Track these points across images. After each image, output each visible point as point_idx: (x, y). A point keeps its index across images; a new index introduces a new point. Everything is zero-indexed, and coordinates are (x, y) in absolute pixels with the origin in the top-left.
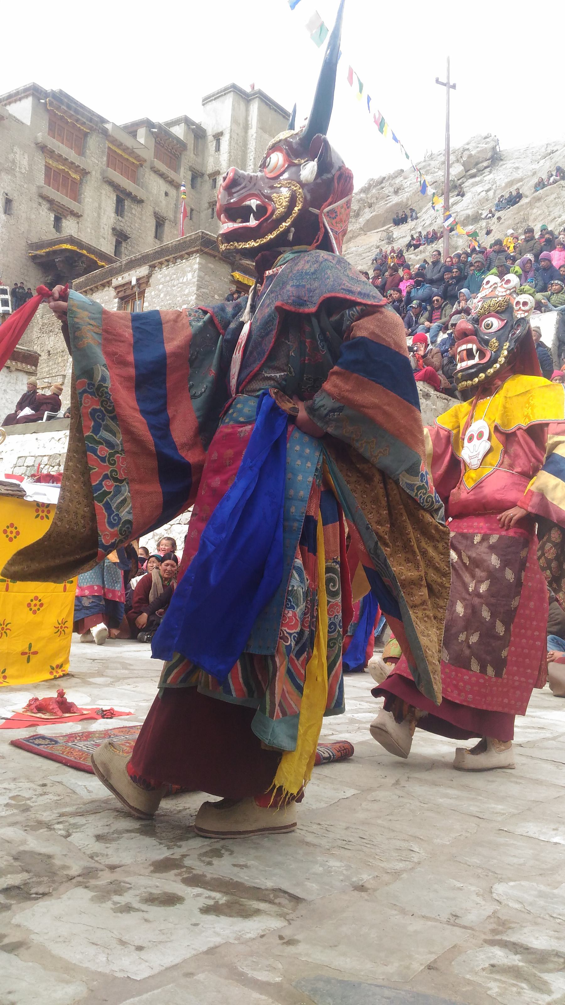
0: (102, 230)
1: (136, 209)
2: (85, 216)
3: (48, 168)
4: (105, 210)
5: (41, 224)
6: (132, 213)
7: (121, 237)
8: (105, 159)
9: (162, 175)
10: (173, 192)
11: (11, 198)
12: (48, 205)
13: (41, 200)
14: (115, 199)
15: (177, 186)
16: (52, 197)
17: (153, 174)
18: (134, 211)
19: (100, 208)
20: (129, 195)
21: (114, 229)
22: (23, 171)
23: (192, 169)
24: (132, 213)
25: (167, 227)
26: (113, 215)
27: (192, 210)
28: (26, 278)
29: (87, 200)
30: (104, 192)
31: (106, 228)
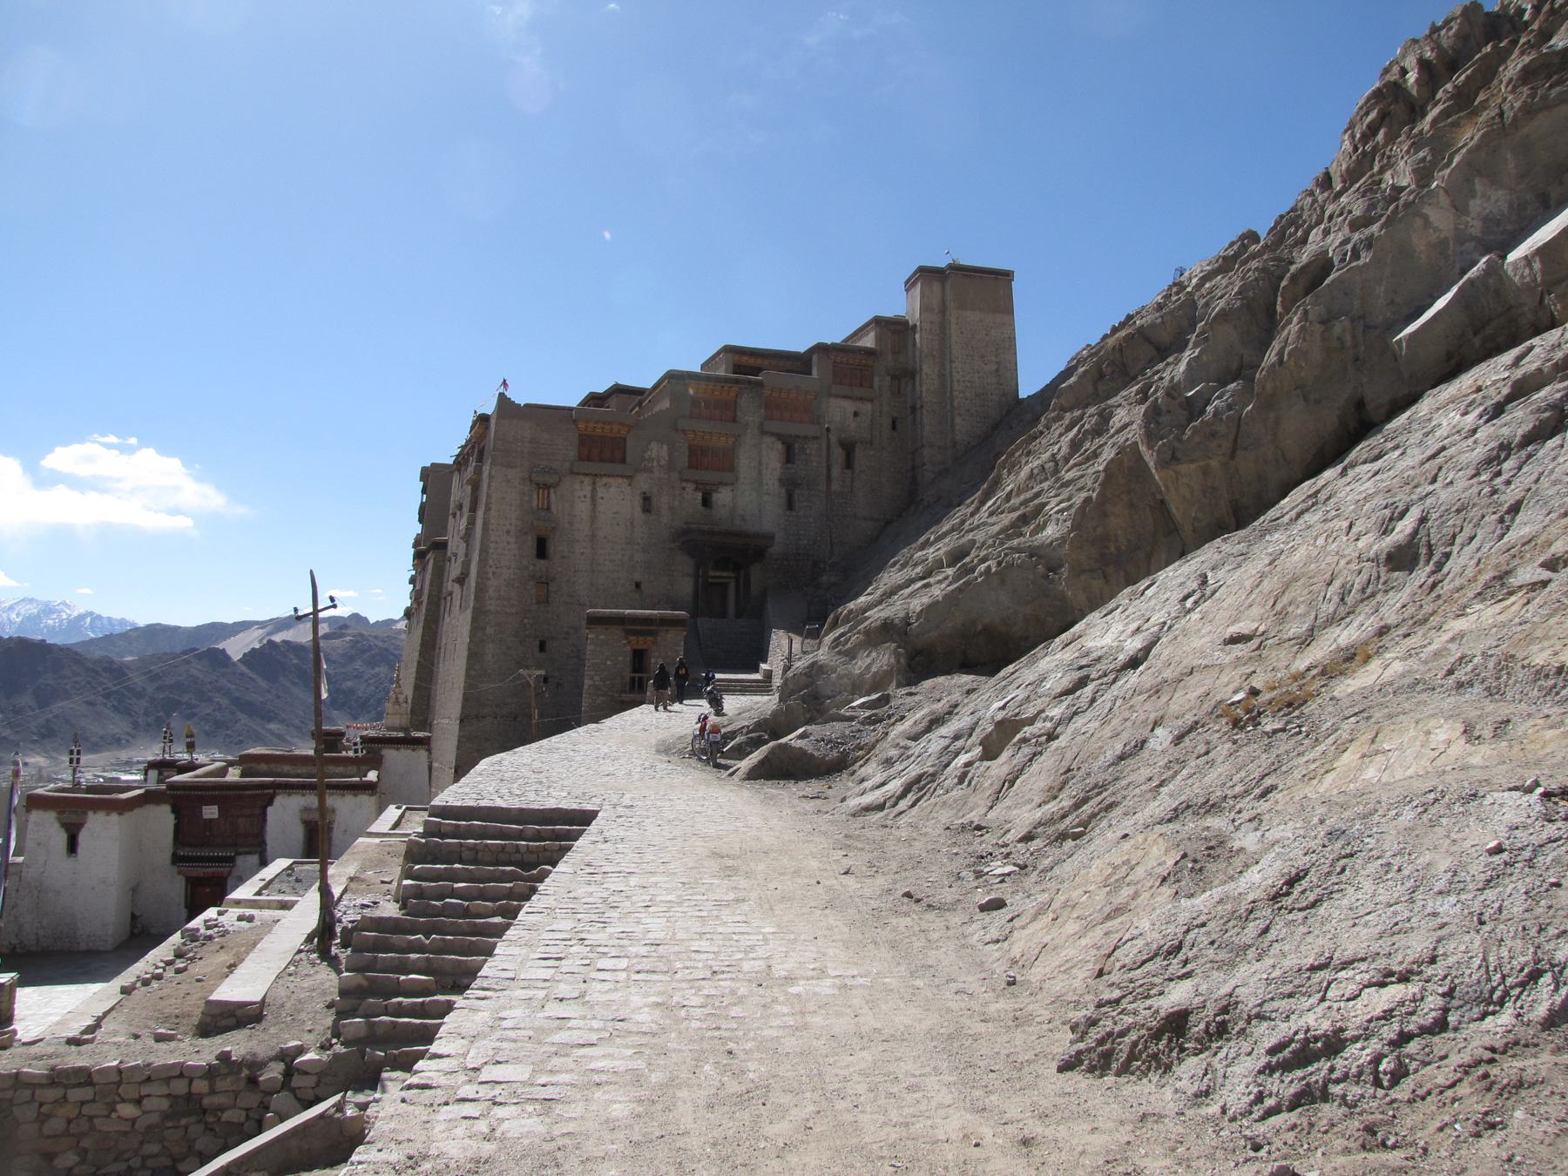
7: (791, 487)
9: (845, 397)
14: (779, 446)
17: (832, 400)
19: (760, 463)
22: (663, 462)
25: (859, 452)
26: (778, 465)
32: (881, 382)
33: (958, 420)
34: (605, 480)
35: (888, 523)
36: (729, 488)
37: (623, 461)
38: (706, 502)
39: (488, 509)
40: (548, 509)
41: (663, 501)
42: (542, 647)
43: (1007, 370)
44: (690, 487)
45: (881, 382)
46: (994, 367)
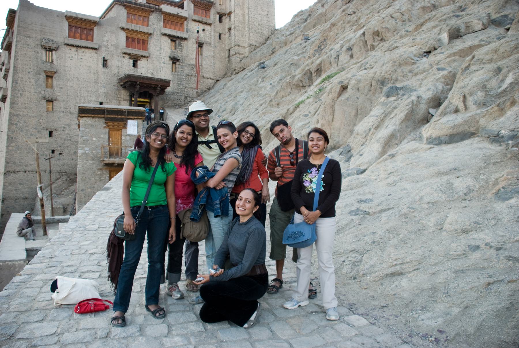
0: (163, 60)
1: (184, 43)
2: (151, 56)
3: (127, 38)
4: (164, 49)
5: (125, 67)
6: (181, 46)
7: (175, 60)
8: (162, 23)
9: (199, 22)
10: (207, 28)
11: (106, 58)
12: (129, 56)
13: (124, 55)
15: (210, 24)
16: (128, 52)
18: (182, 45)
20: (178, 37)
21: (170, 57)
23: (218, 13)
24: (181, 46)
27: (220, 35)
28: (119, 96)
29: (151, 48)
30: (162, 41)
31: (165, 58)
32: (213, 16)
33: (251, 34)
34: (83, 50)
35: (218, 81)
36: (146, 59)
37: (92, 40)
38: (135, 65)
39: (16, 59)
40: (52, 62)
41: (113, 63)
42: (51, 134)
43: (270, 15)
44: (127, 57)
45: (213, 16)
46: (266, 13)
